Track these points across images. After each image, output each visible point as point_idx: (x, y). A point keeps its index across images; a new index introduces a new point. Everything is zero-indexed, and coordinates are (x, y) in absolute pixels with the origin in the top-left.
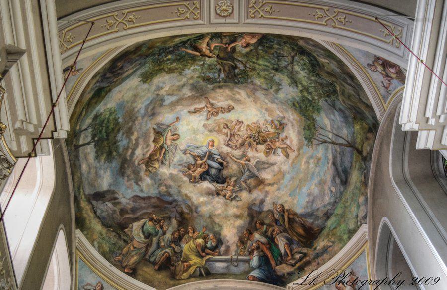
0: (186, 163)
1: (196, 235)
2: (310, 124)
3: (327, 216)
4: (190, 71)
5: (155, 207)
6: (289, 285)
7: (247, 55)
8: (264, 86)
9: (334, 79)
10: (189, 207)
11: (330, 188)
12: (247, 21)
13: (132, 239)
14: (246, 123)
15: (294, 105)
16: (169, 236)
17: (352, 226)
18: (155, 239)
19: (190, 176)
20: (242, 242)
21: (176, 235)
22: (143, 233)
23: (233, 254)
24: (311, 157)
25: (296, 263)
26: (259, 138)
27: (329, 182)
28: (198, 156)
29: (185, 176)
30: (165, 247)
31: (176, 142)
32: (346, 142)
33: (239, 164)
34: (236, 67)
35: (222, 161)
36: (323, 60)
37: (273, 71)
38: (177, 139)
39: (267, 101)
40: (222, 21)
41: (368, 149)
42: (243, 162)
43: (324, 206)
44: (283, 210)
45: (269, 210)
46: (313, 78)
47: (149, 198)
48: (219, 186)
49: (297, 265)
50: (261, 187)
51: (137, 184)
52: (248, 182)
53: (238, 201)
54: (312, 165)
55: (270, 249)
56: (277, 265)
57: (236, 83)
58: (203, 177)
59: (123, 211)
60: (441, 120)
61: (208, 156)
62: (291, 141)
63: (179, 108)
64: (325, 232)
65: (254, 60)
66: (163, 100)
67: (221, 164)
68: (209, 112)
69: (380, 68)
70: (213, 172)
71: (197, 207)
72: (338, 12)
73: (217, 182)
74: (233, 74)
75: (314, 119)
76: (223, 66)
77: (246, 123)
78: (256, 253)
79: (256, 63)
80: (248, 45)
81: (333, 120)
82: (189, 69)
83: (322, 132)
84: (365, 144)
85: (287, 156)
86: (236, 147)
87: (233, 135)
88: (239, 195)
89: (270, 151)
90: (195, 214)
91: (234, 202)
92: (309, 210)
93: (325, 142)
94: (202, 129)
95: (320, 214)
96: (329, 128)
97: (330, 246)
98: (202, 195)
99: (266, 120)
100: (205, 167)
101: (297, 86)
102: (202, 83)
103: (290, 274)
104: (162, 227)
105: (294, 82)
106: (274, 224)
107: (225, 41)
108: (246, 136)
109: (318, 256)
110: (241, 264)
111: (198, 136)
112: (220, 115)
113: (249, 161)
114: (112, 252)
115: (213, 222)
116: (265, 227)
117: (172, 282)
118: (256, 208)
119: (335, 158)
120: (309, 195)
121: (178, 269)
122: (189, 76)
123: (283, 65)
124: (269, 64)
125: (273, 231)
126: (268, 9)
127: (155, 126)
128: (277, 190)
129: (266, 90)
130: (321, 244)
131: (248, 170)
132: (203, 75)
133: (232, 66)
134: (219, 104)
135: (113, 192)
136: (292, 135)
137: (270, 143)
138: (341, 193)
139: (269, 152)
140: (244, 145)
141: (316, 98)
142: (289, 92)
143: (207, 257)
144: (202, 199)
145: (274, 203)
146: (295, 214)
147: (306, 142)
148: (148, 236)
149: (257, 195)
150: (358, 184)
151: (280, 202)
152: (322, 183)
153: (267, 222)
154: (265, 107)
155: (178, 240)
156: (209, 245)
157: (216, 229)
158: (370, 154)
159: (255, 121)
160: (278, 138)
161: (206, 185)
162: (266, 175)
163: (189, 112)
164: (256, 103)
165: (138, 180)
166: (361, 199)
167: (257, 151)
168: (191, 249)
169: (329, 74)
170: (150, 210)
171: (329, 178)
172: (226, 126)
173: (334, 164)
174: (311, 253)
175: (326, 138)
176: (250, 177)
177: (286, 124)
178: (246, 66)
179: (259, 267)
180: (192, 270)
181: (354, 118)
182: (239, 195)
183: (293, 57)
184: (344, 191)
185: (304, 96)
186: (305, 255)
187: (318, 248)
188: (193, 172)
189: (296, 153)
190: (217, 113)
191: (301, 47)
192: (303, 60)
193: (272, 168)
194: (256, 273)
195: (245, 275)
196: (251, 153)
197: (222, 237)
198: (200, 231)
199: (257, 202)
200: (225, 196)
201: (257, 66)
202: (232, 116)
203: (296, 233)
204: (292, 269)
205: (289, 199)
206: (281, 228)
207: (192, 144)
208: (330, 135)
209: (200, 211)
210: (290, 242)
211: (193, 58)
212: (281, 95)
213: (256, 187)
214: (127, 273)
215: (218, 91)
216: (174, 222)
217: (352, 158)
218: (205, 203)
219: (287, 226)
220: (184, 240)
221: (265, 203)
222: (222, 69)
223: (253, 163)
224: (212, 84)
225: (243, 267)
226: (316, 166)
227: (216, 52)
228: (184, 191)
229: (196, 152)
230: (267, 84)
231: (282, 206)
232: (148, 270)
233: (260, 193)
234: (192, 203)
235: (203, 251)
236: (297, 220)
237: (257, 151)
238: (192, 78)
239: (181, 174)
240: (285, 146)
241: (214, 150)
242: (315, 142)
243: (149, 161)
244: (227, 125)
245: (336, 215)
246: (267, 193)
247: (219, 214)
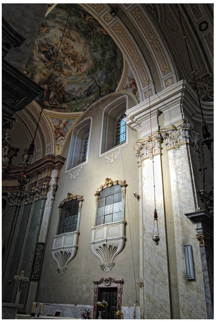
0: (42, 43)
2: (94, 70)
3: (74, 99)
4: (74, 18)
7: (98, 34)
8: (92, 46)
9: (115, 67)
11: (81, 93)
12: (110, 29)
14: (74, 49)
15: (95, 60)
17: (78, 109)
19: (40, 48)
24: (85, 79)
25: (52, 104)
26: (74, 57)
27: (83, 91)
28: (49, 45)
29: (38, 47)
31: (46, 34)
32: (99, 86)
34: (90, 32)
35: (55, 53)
36: (118, 60)
37: (100, 45)
38: (47, 33)
39: (88, 50)
40: (104, 20)
41: (104, 94)
42: (62, 60)
43: (75, 96)
45: (57, 82)
46: (109, 60)
48: (47, 60)
49: (52, 106)
50: (60, 72)
53: (49, 70)
54: (82, 81)
57: (84, 36)
58: (44, 52)
60: (136, 122)
61: (52, 48)
62: (83, 68)
63: (58, 24)
64: (69, 103)
65: (98, 37)
66: (55, 17)
67: (54, 54)
68: (66, 35)
69: (131, 82)
70: (49, 54)
71: (33, 60)
72: (138, 57)
73: (47, 58)
74: (86, 33)
75: (96, 70)
76: (86, 28)
77: (74, 49)
79: (98, 38)
80: (102, 32)
81: (102, 77)
82: (75, 17)
83: (95, 76)
84: (105, 92)
85: (77, 71)
86: (64, 53)
87: (67, 49)
89: (73, 64)
90: (31, 62)
91: (47, 69)
92: (69, 93)
93: (93, 79)
94: (58, 37)
95: (72, 97)
96: (99, 77)
97: (67, 109)
98: (38, 58)
99: (82, 55)
100: (47, 50)
101: (102, 57)
102: (74, 25)
105: (103, 55)
106: (54, 87)
107: (96, 23)
108: (70, 53)
109: (60, 108)
111: (55, 38)
112: (69, 39)
113: (64, 61)
115: (35, 69)
116: (51, 85)
119: (91, 86)
120: (73, 89)
122: (72, 19)
123: (105, 48)
124: (101, 42)
125: (53, 89)
126: (120, 32)
127: (44, 22)
128: (65, 78)
129: (91, 47)
130: (64, 105)
131: (61, 63)
132: (77, 23)
133: (89, 31)
134: (72, 36)
136: (85, 67)
137: (76, 62)
138: (84, 97)
139: (73, 65)
140: (67, 55)
141: (104, 66)
142: (98, 55)
144: (37, 59)
145: (60, 81)
146: (64, 90)
147: (87, 73)
149: (57, 73)
150: (91, 100)
152: (81, 89)
154: (85, 51)
157: (34, 73)
158: (103, 96)
159: (78, 51)
160: (80, 63)
161: (43, 56)
162: (65, 71)
163: (60, 28)
164: (84, 47)
166: (88, 104)
167: (69, 61)
169: (116, 66)
171: (84, 90)
172: (67, 44)
173: (90, 87)
174: (59, 106)
175: (95, 79)
176: (59, 66)
177: (87, 63)
178: (93, 35)
181: (109, 83)
183: (110, 49)
184: (85, 97)
185: (101, 61)
187: (63, 106)
188: (42, 48)
189: (81, 73)
190: (68, 38)
191: (116, 51)
192: (113, 53)
193: (69, 70)
196: (66, 59)
197: (34, 77)
200: (46, 65)
201: (97, 39)
202: (72, 43)
203: (59, 96)
204: (49, 105)
205: (66, 84)
206: (56, 90)
207: (50, 39)
208: (97, 79)
209: (33, 62)
210: (55, 97)
211: (80, 17)
212: (94, 54)
213: (58, 71)
215: (76, 32)
217: (96, 91)
218: (37, 61)
219: (58, 91)
221: (57, 78)
222: (85, 28)
223: (65, 63)
224: (76, 28)
226: (83, 83)
227: (89, 22)
230: (94, 46)
231: (62, 84)
233: (58, 74)
234: (33, 57)
236: (63, 92)
237: (69, 61)
238: (72, 20)
239: (37, 45)
240: (80, 68)
241: (56, 47)
242: (90, 76)
244: (68, 44)
245: (76, 102)
246: (61, 76)
247: (39, 69)
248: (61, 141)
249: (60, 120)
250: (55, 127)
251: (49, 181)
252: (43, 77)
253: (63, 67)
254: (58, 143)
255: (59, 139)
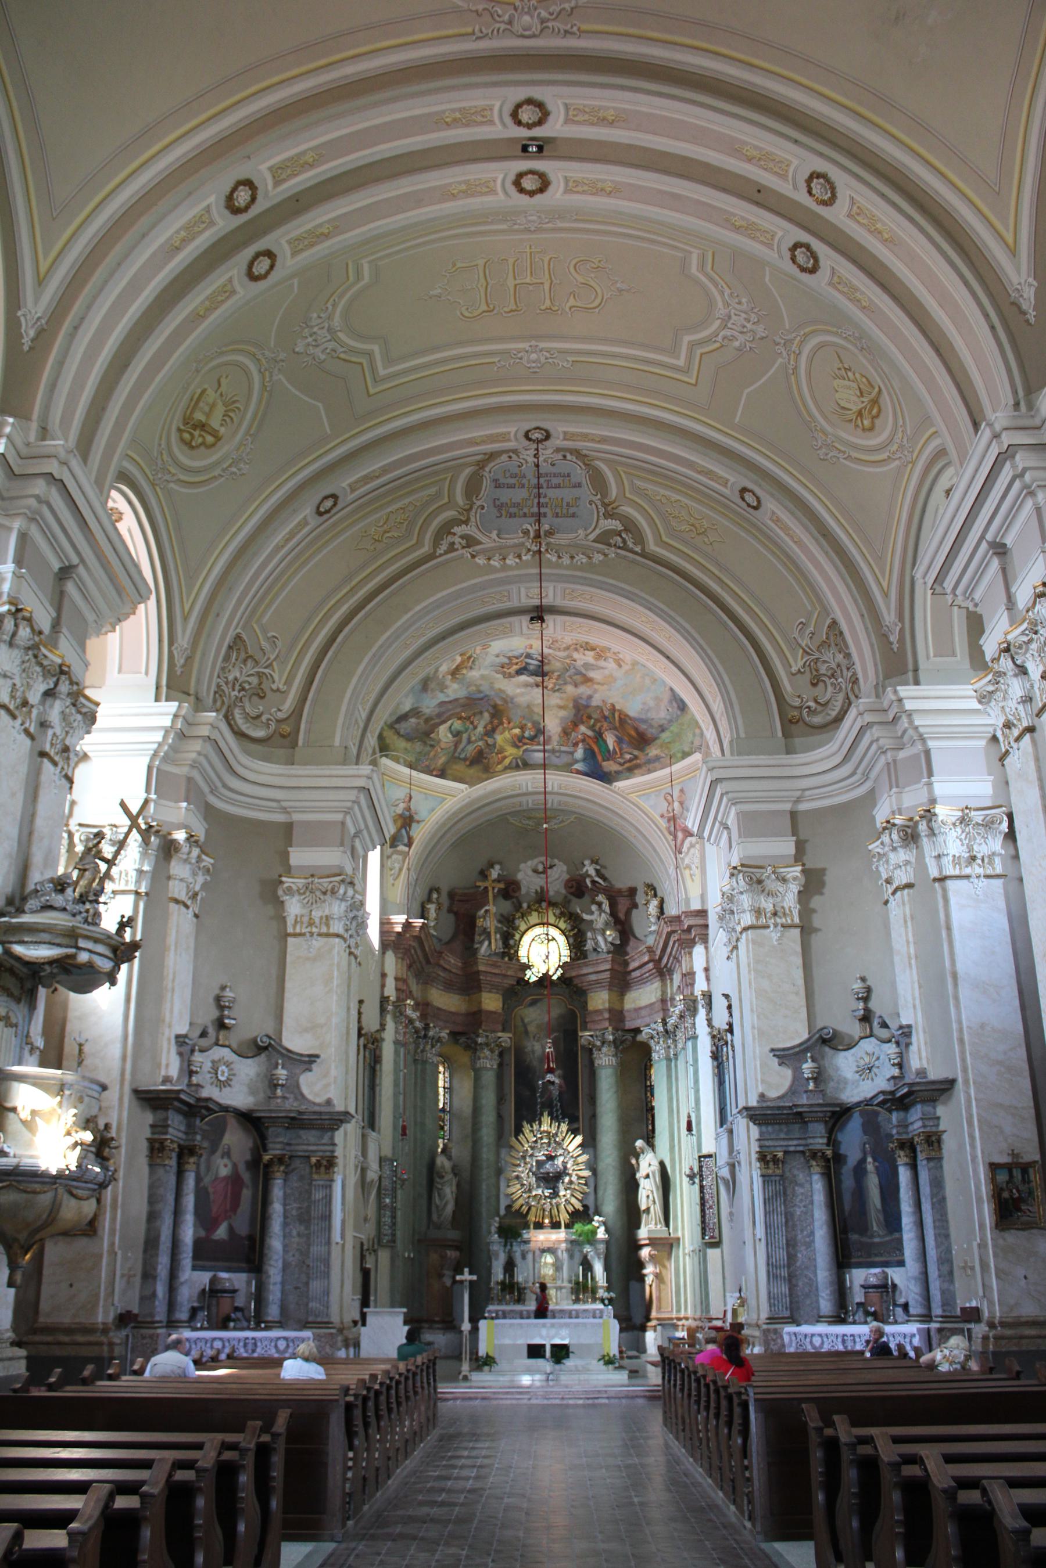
1: (512, 724)
3: (663, 729)
5: (463, 706)
6: (615, 784)
10: (505, 701)
13: (439, 741)
16: (480, 729)
17: (687, 749)
18: (465, 736)
19: (504, 674)
20: (566, 733)
21: (489, 727)
22: (451, 732)
23: (554, 744)
25: (625, 763)
30: (476, 741)
33: (563, 663)
44: (613, 709)
47: (456, 700)
50: (589, 684)
51: (442, 691)
52: (575, 677)
55: (596, 742)
56: (604, 760)
58: (519, 672)
59: (427, 721)
64: (658, 741)
71: (512, 699)
78: (580, 745)
88: (564, 687)
90: (510, 705)
91: (557, 694)
92: (644, 717)
103: (617, 773)
104: (472, 723)
109: (649, 762)
110: (563, 755)
114: (417, 760)
116: (592, 721)
117: (484, 776)
118: (584, 702)
120: (644, 704)
121: (491, 761)
130: (653, 751)
135: (416, 708)
138: (678, 716)
143: (525, 747)
144: (518, 691)
146: (627, 716)
148: (457, 734)
149: (583, 690)
151: (611, 701)
153: (595, 716)
155: (490, 732)
156: (527, 734)
161: (524, 678)
165: (442, 688)
168: (506, 740)
170: (458, 710)
179: (584, 760)
180: (507, 762)
182: (564, 687)
186: (636, 757)
194: (579, 766)
195: (567, 768)
196: (576, 655)
198: (516, 720)
199: (584, 697)
210: (619, 741)
213: (583, 683)
214: (436, 776)
216: (486, 715)
218: (522, 694)
219: (617, 724)
220: (497, 731)
225: (565, 759)
228: (497, 686)
229: (510, 654)
231: (613, 706)
232: (459, 768)
234: (507, 695)
235: (520, 741)
243: (455, 673)
245: (672, 732)
246: (596, 691)
248: (692, 851)
249: (664, 792)
250: (662, 816)
251: (692, 985)
252: (563, 713)
253: (584, 671)
254: (687, 861)
255: (685, 849)
